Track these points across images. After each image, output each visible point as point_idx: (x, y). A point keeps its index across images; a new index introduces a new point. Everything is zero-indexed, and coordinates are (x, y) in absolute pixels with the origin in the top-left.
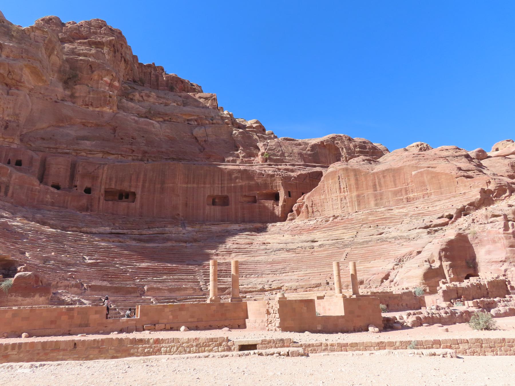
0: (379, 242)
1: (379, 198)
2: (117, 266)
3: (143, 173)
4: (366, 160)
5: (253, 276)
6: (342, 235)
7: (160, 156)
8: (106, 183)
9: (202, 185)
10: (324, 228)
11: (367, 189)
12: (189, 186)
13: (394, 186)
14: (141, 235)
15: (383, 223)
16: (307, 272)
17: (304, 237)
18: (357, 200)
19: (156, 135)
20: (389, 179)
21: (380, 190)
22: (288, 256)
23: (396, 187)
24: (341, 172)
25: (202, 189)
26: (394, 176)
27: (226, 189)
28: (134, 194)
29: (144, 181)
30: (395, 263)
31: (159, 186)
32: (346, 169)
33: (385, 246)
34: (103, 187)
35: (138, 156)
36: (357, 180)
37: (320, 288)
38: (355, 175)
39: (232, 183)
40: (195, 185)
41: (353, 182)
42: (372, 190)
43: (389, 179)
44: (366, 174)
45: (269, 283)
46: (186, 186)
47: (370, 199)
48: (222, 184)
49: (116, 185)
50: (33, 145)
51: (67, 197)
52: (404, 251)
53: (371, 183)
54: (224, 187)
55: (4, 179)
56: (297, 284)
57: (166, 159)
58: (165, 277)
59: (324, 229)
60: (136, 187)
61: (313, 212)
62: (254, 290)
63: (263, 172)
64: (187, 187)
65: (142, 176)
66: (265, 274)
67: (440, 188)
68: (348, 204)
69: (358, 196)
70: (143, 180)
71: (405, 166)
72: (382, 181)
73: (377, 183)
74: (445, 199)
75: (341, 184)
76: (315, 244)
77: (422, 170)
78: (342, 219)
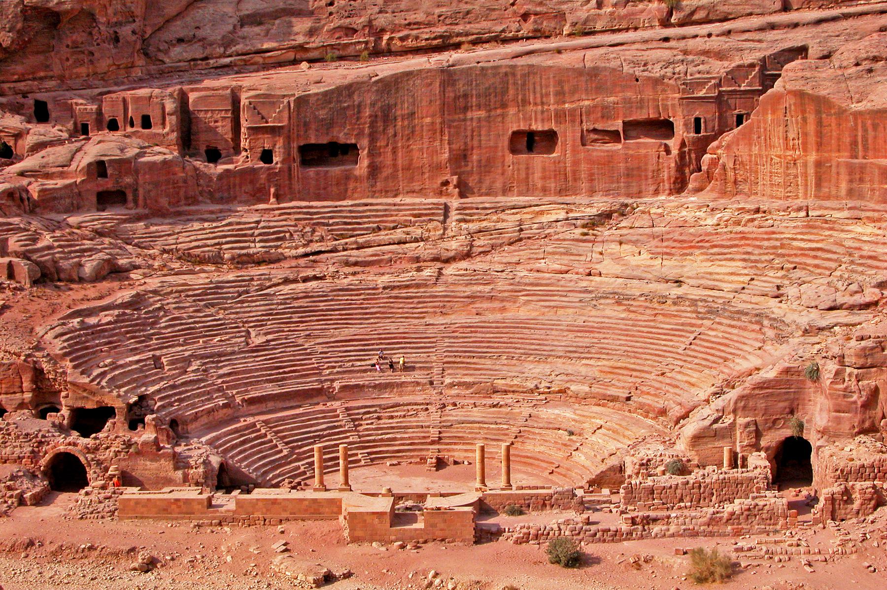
1: (857, 175)
2: (300, 341)
4: (866, 59)
5: (531, 358)
6: (727, 278)
7: (414, 32)
8: (298, 136)
9: (499, 111)
10: (715, 246)
11: (839, 151)
12: (469, 115)
14: (363, 247)
15: (805, 264)
16: (619, 364)
17: (670, 267)
18: (816, 173)
21: (864, 158)
22: (616, 313)
24: (790, 101)
25: (500, 119)
28: (354, 147)
30: (713, 389)
31: (406, 123)
32: (800, 95)
34: (295, 145)
35: (366, 43)
36: (820, 123)
38: (818, 112)
39: (564, 103)
40: (482, 114)
41: (811, 128)
44: (842, 113)
45: (551, 378)
46: (461, 116)
48: (543, 104)
50: (167, 60)
51: (232, 179)
53: (847, 140)
54: (548, 110)
55: (128, 180)
56: (587, 389)
57: (427, 39)
59: (715, 250)
61: (735, 182)
62: (521, 390)
65: (367, 112)
66: (553, 356)
69: (818, 164)
70: (370, 116)
72: (871, 133)
75: (790, 128)
76: (676, 291)
78: (760, 227)
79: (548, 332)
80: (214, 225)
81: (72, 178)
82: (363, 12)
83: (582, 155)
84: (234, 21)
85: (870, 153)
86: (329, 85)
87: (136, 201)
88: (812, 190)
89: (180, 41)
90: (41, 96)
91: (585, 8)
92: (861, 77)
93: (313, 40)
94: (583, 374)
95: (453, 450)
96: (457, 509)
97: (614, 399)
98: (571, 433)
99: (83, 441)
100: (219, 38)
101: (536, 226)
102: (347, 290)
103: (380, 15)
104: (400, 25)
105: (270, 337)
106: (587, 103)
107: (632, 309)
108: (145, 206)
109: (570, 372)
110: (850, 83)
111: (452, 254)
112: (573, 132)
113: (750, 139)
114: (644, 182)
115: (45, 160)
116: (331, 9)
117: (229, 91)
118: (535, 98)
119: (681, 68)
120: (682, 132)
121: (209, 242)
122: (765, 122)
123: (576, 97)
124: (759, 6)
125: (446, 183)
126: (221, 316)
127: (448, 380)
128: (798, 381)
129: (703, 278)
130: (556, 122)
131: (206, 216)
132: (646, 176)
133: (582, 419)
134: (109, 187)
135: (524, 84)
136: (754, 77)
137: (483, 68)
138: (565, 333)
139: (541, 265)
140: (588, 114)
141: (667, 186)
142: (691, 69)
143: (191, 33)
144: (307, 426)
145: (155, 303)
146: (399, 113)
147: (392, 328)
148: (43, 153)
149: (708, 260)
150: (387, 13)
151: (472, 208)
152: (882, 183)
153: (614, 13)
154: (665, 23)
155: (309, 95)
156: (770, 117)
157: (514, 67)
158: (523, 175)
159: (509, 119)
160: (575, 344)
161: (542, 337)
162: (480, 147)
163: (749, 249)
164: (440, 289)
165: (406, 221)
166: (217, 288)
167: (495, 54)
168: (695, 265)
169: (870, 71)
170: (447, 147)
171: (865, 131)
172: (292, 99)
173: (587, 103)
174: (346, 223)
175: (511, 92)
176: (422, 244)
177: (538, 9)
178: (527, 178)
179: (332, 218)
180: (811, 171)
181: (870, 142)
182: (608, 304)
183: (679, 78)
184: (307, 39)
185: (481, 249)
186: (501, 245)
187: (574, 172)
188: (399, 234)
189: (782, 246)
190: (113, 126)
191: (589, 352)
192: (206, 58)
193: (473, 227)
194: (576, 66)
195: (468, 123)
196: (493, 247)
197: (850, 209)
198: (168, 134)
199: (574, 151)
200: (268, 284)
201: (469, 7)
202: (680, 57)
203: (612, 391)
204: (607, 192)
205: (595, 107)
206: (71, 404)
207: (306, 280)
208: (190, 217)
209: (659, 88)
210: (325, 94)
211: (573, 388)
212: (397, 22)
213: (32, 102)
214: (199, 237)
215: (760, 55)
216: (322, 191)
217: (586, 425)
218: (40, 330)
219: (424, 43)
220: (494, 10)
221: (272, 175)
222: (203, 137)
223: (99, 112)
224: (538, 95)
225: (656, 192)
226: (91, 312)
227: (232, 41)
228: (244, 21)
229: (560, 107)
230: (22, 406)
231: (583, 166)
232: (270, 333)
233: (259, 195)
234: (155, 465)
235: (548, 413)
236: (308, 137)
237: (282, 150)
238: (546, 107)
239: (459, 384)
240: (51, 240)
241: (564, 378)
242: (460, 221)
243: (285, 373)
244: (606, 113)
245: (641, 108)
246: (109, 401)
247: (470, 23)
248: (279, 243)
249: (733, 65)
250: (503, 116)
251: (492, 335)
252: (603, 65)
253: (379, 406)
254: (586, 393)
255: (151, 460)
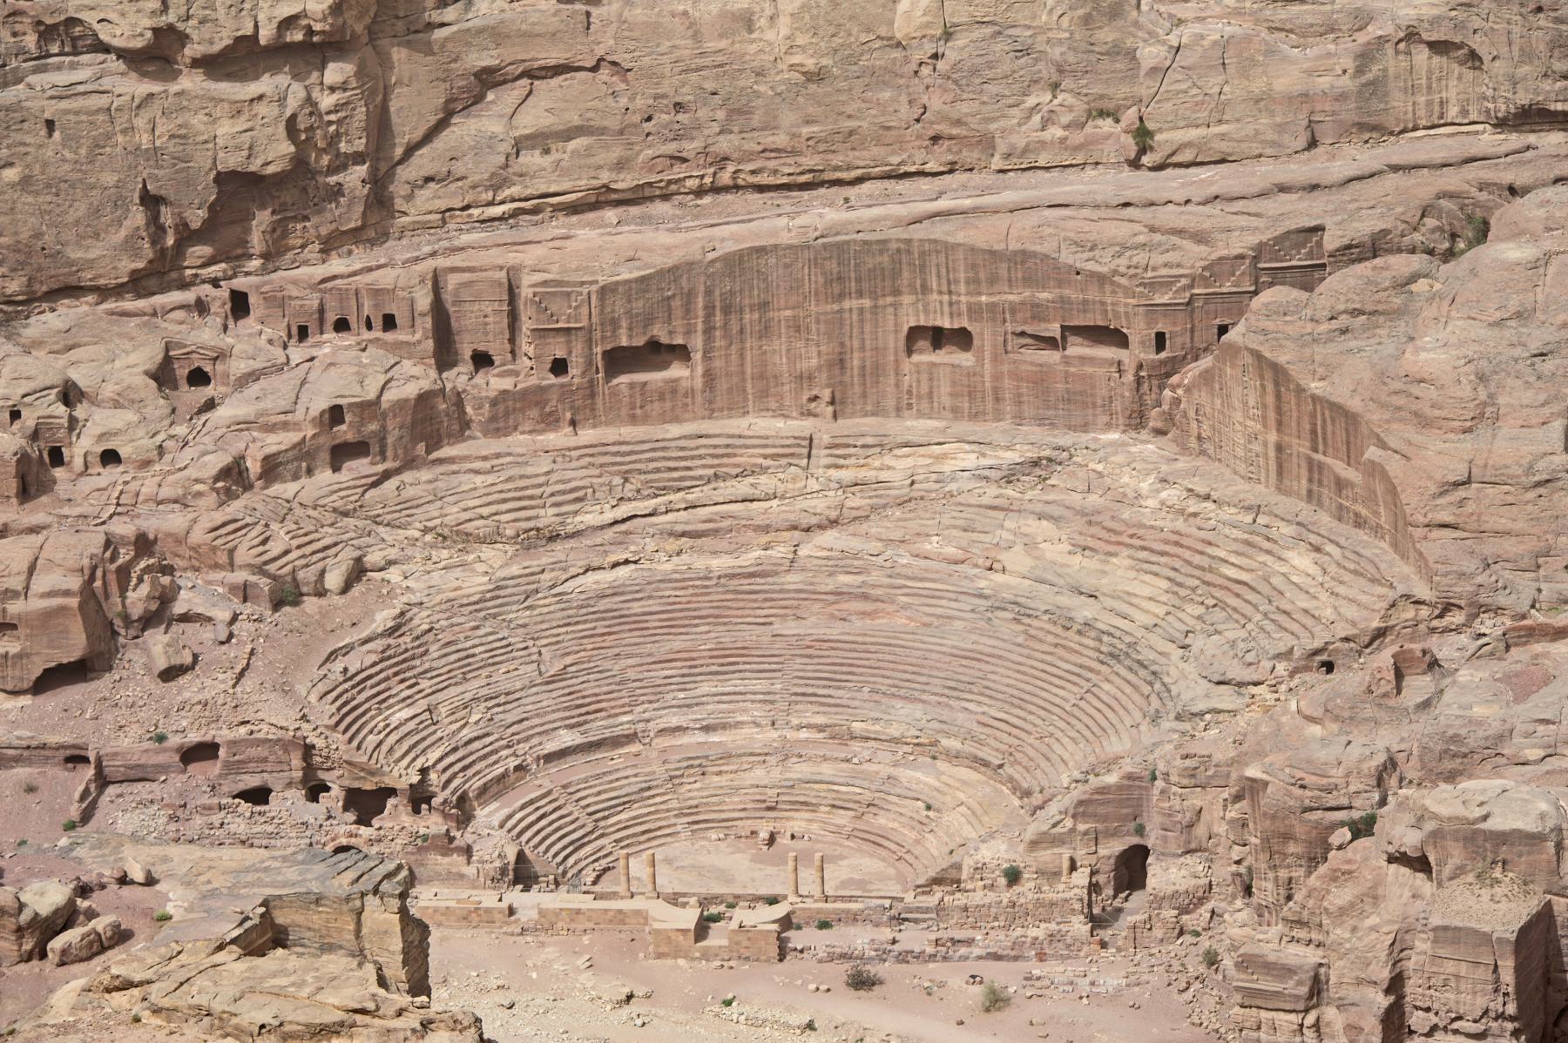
2: (607, 665)
3: (702, 288)
7: (772, 164)
9: (889, 299)
12: (847, 304)
19: (760, 73)
21: (1324, 454)
24: (1249, 360)
25: (890, 310)
27: (964, 308)
29: (709, 310)
31: (756, 316)
32: (1258, 356)
34: (599, 350)
35: (702, 177)
36: (1278, 397)
38: (1277, 384)
39: (980, 294)
40: (866, 303)
41: (1270, 400)
42: (1308, 444)
44: (1300, 390)
46: (836, 307)
48: (950, 292)
49: (630, 337)
54: (958, 302)
55: (373, 427)
58: (705, 688)
59: (1144, 555)
60: (688, 332)
63: (1079, 260)
64: (841, 311)
69: (1279, 448)
70: (706, 307)
72: (1329, 428)
79: (928, 654)
80: (491, 479)
81: (300, 430)
82: (695, 133)
83: (1005, 368)
84: (507, 147)
86: (647, 266)
87: (383, 453)
89: (428, 179)
90: (240, 283)
91: (1024, 128)
92: (1330, 340)
93: (622, 176)
94: (959, 722)
95: (792, 819)
96: (760, 927)
97: (986, 764)
98: (929, 808)
99: (364, 831)
100: (486, 176)
101: (934, 476)
102: (670, 581)
103: (721, 138)
104: (752, 153)
105: (569, 660)
106: (1011, 297)
107: (1032, 632)
108: (396, 457)
109: (944, 718)
110: (1318, 349)
111: (814, 520)
112: (994, 334)
114: (1090, 411)
115: (262, 405)
116: (648, 126)
117: (503, 274)
118: (939, 285)
119: (1141, 258)
120: (1139, 352)
121: (485, 511)
123: (996, 288)
124: (1273, 144)
125: (815, 398)
126: (505, 633)
127: (795, 721)
128: (1140, 787)
129: (1119, 598)
130: (970, 319)
131: (478, 465)
132: (1094, 404)
133: (946, 789)
134: (344, 437)
135: (923, 266)
136: (1243, 273)
137: (865, 242)
138: (948, 659)
139: (932, 545)
140: (1013, 311)
141: (1121, 421)
142: (1158, 259)
143: (445, 169)
144: (614, 789)
145: (421, 621)
146: (747, 301)
147: (727, 640)
148: (254, 389)
149: (1132, 568)
150: (731, 132)
151: (848, 446)
153: (1066, 138)
154: (1135, 164)
155: (617, 283)
156: (1229, 371)
157: (909, 241)
158: (924, 389)
159: (902, 312)
160: (956, 677)
161: (919, 661)
162: (862, 348)
163: (1178, 564)
164: (793, 580)
165: (754, 465)
166: (498, 588)
167: (885, 218)
168: (1119, 574)
169: (1344, 331)
170: (814, 349)
171: (1324, 421)
172: (594, 288)
173: (1011, 297)
174: (670, 469)
175: (906, 274)
176: (775, 503)
177: (954, 132)
178: (931, 393)
179: (651, 460)
180: (1272, 454)
181: (1329, 435)
183: (1135, 275)
184: (614, 176)
185: (855, 513)
186: (885, 506)
187: (996, 390)
188: (743, 487)
190: (342, 325)
191: (971, 692)
192: (468, 207)
193: (846, 475)
194: (996, 248)
195: (847, 315)
196: (873, 508)
198: (419, 342)
199: (995, 359)
200: (564, 577)
201: (852, 124)
202: (1141, 239)
203: (984, 753)
204: (1041, 421)
205: (1023, 303)
206: (347, 783)
207: (615, 565)
208: (455, 467)
209: (1108, 288)
210: (642, 279)
211: (945, 742)
212: (746, 147)
213: (227, 294)
214: (471, 503)
215: (1253, 240)
216: (638, 411)
217: (948, 799)
218: (301, 689)
219: (785, 180)
220: (889, 128)
221: (566, 391)
222: (467, 337)
223: (321, 311)
224: (944, 281)
225: (1109, 426)
226: (348, 649)
227: (505, 180)
228: (519, 146)
229: (973, 299)
230: (289, 785)
231: (1007, 383)
232: (568, 654)
233: (550, 421)
234: (447, 860)
235: (906, 775)
236: (615, 335)
237: (581, 360)
238: (954, 298)
239: (809, 726)
240: (287, 538)
241: (937, 725)
242: (828, 467)
243: (588, 713)
244: (1038, 312)
245: (1085, 311)
246: (388, 782)
247: (853, 149)
248: (577, 506)
249: (1214, 256)
250: (896, 306)
251: (856, 655)
252: (1033, 248)
253: (706, 757)
255: (443, 855)
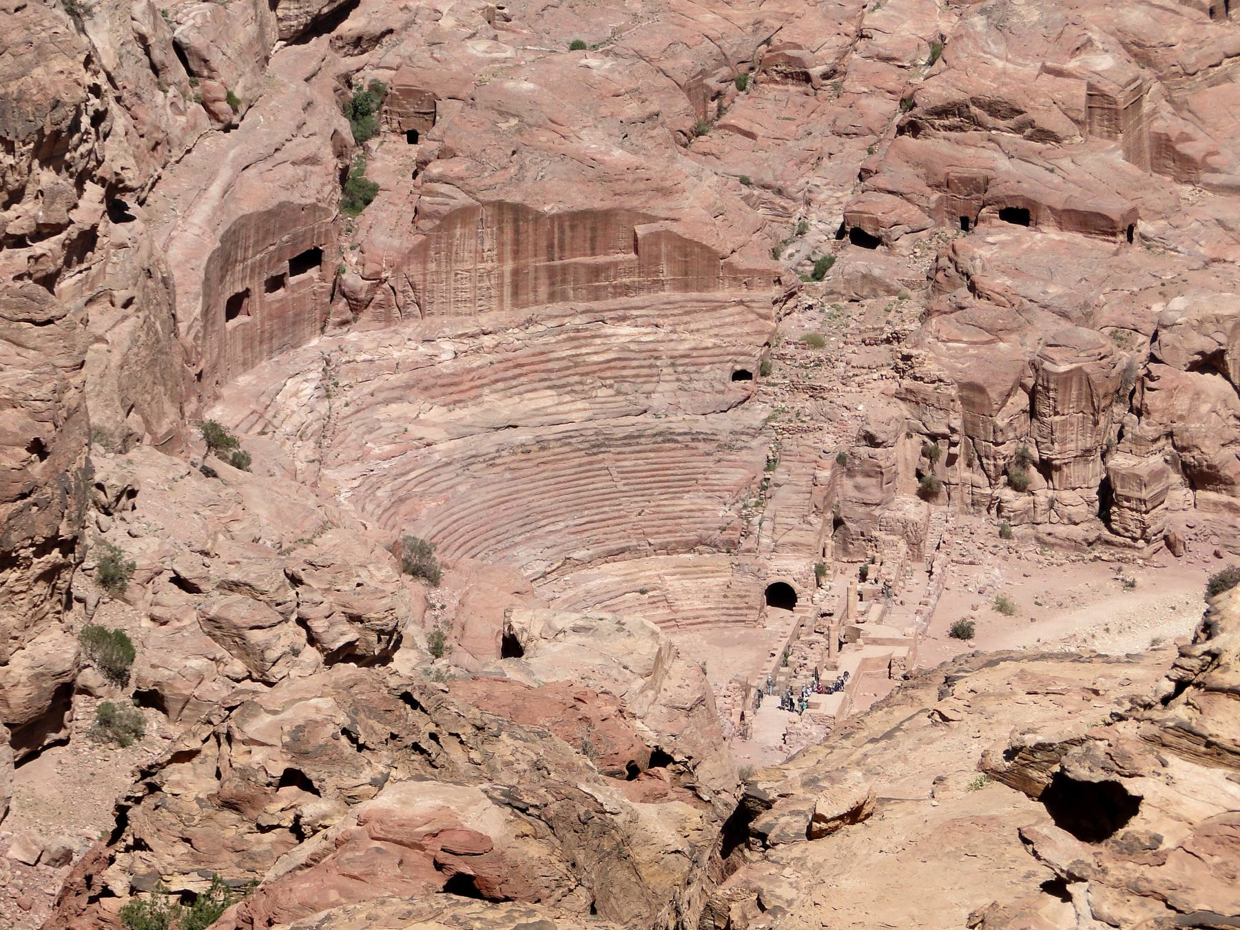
0: (660, 439)
1: (556, 277)
13: (589, 252)
15: (623, 377)
20: (583, 232)
21: (561, 259)
23: (593, 254)
24: (486, 213)
26: (593, 229)
32: (500, 206)
33: (678, 453)
36: (517, 231)
37: (627, 555)
38: (516, 220)
41: (508, 236)
43: (583, 232)
44: (539, 216)
47: (540, 281)
52: (735, 476)
53: (543, 243)
59: (500, 385)
67: (686, 274)
68: (493, 292)
69: (516, 273)
71: (622, 209)
72: (568, 233)
73: (556, 242)
74: (707, 311)
77: (656, 227)
85: (567, 253)
88: (508, 300)
113: (426, 256)
122: (452, 237)
152: (590, 281)
171: (562, 232)
180: (508, 279)
181: (567, 241)
182: (482, 469)
189: (576, 365)
197: (583, 312)
254: (591, 556)
